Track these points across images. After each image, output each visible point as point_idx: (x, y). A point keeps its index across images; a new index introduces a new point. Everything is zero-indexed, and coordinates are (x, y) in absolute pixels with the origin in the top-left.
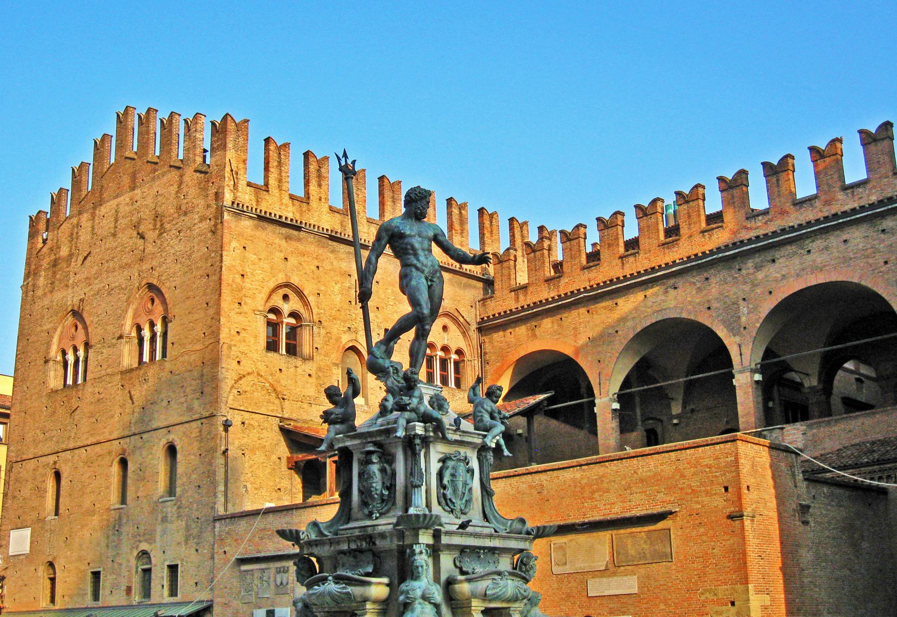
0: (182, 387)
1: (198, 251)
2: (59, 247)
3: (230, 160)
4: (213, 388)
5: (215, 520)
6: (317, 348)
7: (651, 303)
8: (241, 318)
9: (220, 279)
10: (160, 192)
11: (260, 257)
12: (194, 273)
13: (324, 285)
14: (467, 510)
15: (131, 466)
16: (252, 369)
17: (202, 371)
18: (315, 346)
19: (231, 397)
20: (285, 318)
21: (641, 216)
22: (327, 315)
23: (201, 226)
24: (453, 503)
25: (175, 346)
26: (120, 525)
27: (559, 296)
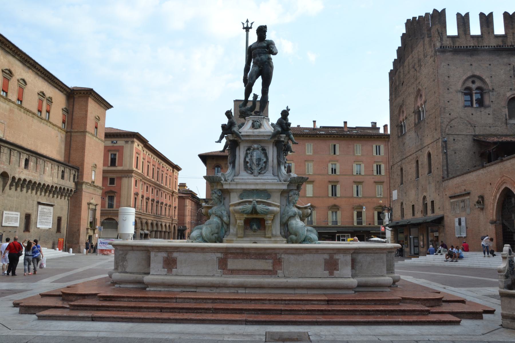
0: (431, 128)
2: (396, 82)
6: (492, 101)
15: (420, 163)
19: (447, 129)
24: (252, 169)
26: (418, 186)
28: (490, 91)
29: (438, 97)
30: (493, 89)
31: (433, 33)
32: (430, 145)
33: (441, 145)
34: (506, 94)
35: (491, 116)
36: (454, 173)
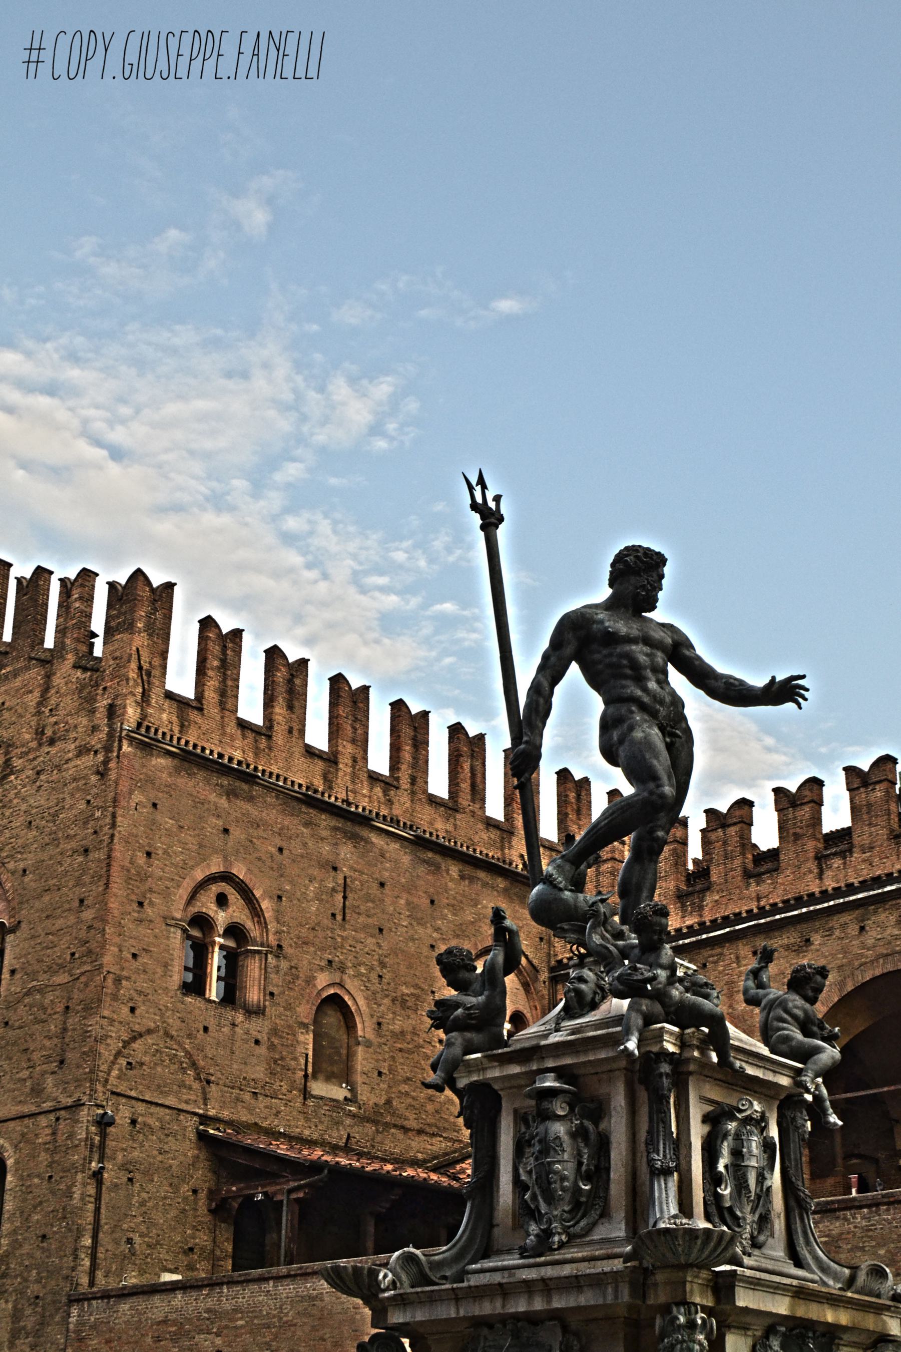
0: (26, 1050)
1: (71, 807)
3: (138, 649)
4: (84, 1053)
5: (72, 1301)
6: (272, 994)
7: (873, 940)
8: (143, 930)
9: (109, 857)
10: (7, 705)
11: (181, 824)
12: (61, 846)
13: (291, 882)
14: (762, 1238)
16: (154, 1022)
17: (65, 1023)
18: (271, 988)
19: (115, 1073)
20: (219, 936)
21: (856, 786)
22: (292, 935)
23: (79, 762)
24: (736, 1218)
25: (18, 976)
27: (701, 924)
28: (271, 952)
29: (97, 924)
30: (280, 947)
31: (115, 659)
32: (11, 1124)
33: (84, 1135)
34: (315, 978)
35: (262, 1050)
36: (114, 1268)
